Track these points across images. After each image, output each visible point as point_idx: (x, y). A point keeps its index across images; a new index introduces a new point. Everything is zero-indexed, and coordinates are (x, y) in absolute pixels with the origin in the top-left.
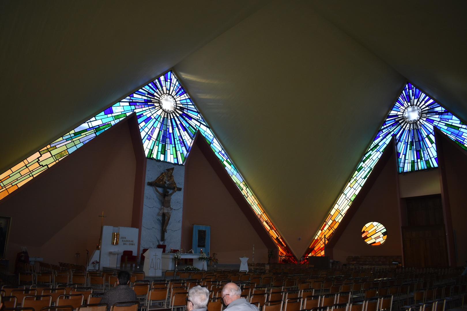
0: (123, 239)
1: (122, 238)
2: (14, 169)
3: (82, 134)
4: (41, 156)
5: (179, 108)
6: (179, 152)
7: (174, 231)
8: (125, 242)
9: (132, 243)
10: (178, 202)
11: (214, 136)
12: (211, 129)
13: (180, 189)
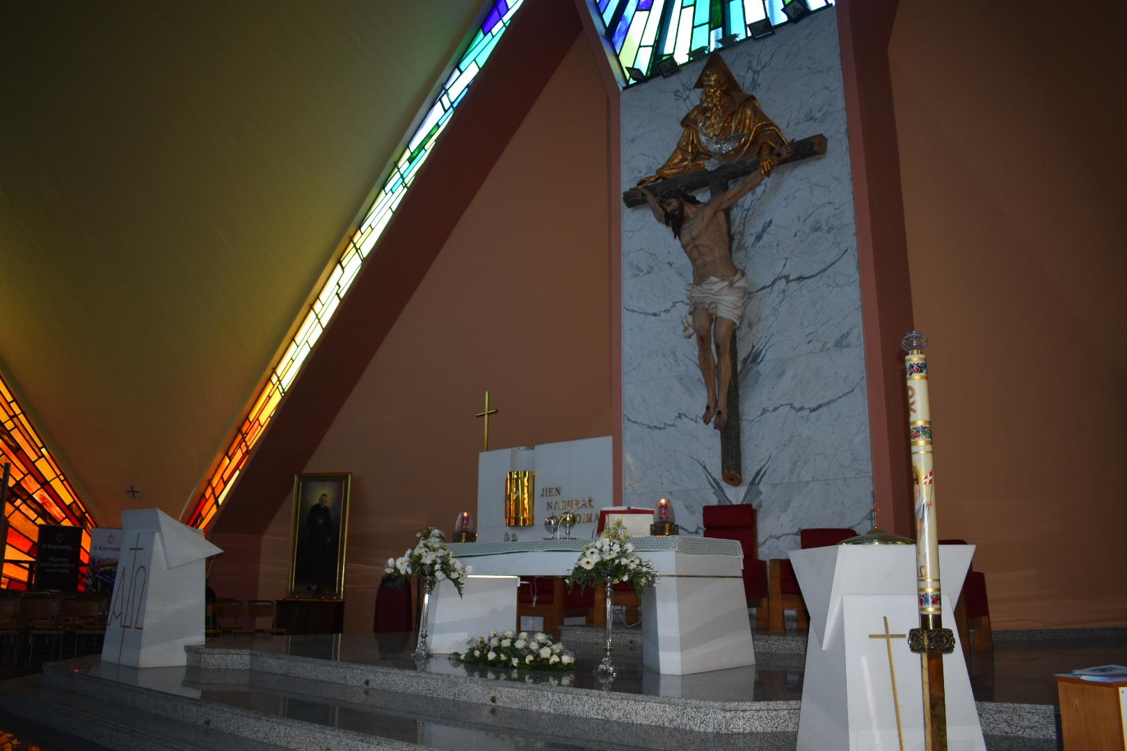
0: (549, 499)
10: (817, 229)
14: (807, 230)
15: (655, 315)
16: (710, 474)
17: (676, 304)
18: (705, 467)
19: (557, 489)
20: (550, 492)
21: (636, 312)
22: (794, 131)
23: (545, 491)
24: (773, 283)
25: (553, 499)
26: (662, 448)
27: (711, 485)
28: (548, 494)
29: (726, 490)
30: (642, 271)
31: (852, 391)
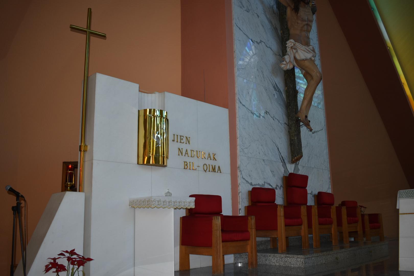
1: (180, 139)
8: (188, 160)
16: (280, 153)
17: (259, 41)
18: (278, 149)
19: (187, 138)
20: (181, 139)
21: (242, 31)
23: (176, 136)
25: (184, 147)
26: (259, 129)
27: (281, 160)
28: (179, 140)
29: (287, 165)
30: (244, 7)
31: (322, 129)
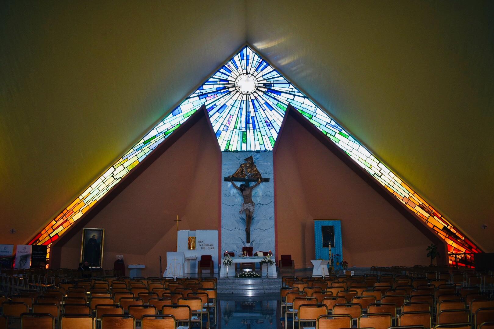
2: (93, 186)
3: (151, 141)
4: (115, 170)
5: (262, 85)
6: (266, 136)
7: (264, 230)
8: (202, 247)
9: (212, 247)
10: (267, 196)
11: (316, 106)
12: (309, 99)
13: (267, 180)
14: (265, 195)
15: (230, 206)
18: (241, 239)
22: (264, 176)
24: (257, 204)
